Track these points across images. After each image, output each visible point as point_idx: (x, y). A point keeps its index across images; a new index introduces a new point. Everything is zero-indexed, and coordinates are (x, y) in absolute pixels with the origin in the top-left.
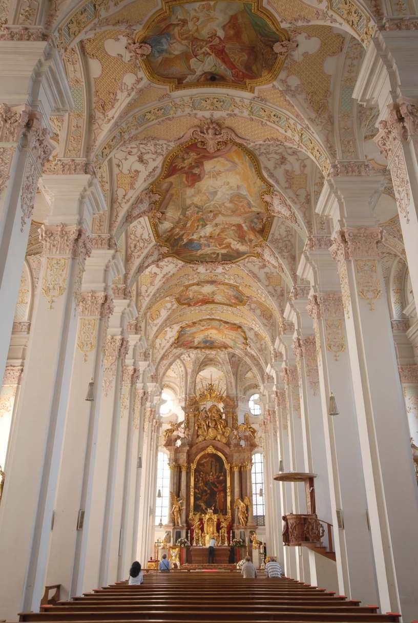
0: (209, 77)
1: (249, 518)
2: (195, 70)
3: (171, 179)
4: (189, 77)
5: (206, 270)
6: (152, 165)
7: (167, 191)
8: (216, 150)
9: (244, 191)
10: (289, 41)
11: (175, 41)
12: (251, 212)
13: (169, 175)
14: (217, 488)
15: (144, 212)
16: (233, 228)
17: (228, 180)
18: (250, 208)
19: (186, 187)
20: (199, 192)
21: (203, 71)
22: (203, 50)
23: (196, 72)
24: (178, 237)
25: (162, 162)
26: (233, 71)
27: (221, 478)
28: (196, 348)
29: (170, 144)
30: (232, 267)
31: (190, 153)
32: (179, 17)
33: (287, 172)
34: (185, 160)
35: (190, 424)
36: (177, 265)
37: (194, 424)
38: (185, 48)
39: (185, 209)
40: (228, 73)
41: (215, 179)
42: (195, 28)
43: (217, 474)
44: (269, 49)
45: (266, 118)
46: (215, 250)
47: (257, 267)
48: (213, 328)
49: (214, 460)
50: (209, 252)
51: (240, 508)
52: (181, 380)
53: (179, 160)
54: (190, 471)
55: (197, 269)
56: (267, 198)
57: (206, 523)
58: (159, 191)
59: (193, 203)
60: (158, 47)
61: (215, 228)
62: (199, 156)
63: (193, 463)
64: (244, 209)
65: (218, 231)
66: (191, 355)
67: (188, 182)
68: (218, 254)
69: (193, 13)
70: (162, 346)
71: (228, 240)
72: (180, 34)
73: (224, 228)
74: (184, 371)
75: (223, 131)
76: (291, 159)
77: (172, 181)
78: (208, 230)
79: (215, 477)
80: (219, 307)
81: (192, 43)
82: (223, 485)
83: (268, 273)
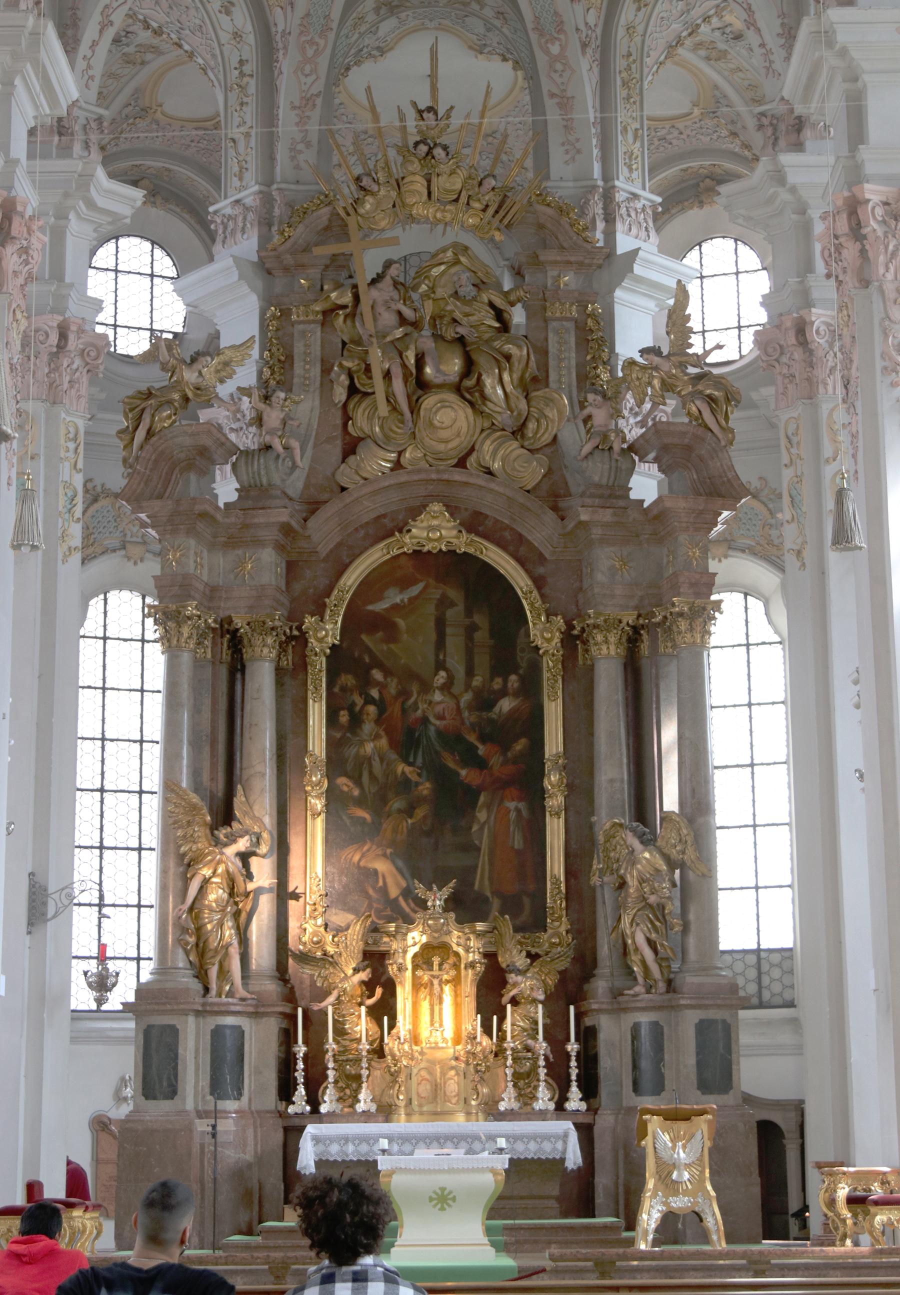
1: (691, 941)
14: (481, 764)
27: (506, 705)
35: (298, 368)
37: (326, 370)
43: (477, 681)
49: (455, 594)
51: (632, 883)
52: (233, 97)
54: (302, 665)
57: (409, 974)
63: (320, 610)
74: (251, 39)
79: (467, 697)
82: (520, 745)
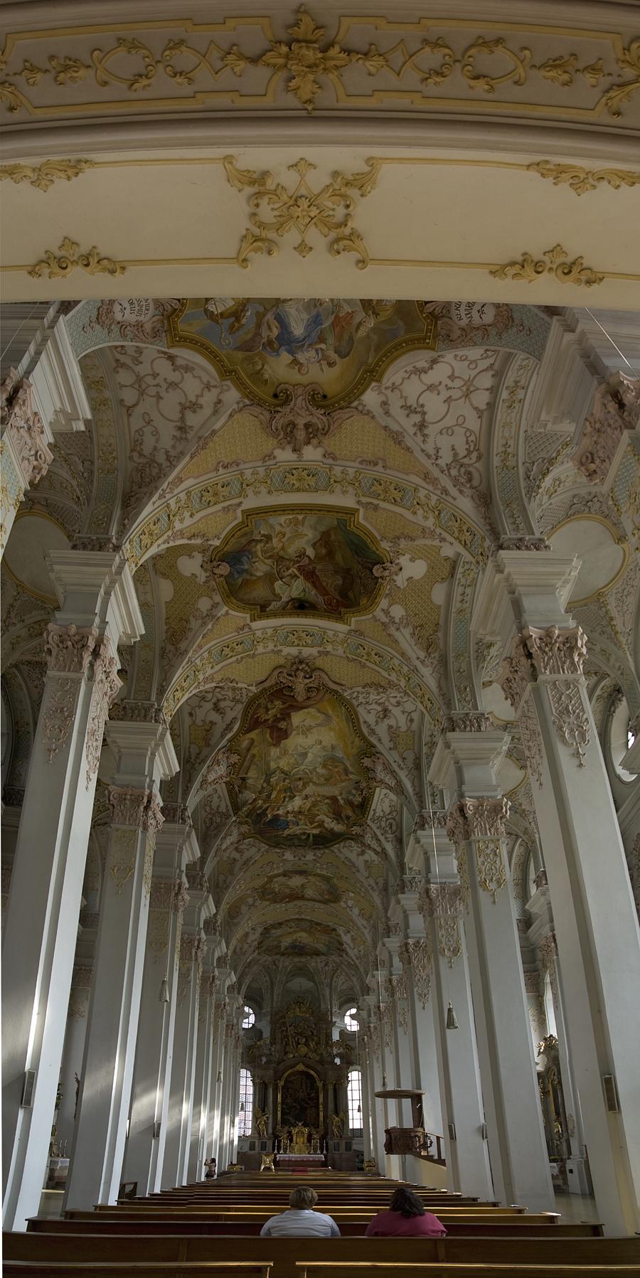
0: (297, 605)
2: (282, 595)
3: (253, 735)
4: (274, 603)
5: (295, 857)
6: (230, 715)
7: (249, 750)
10: (391, 563)
11: (257, 559)
12: (349, 780)
13: (249, 731)
15: (221, 777)
16: (326, 801)
17: (321, 738)
19: (270, 746)
20: (285, 752)
21: (290, 596)
22: (290, 571)
23: (281, 598)
24: (260, 811)
26: (325, 597)
28: (283, 954)
29: (250, 688)
32: (262, 532)
33: (390, 727)
36: (259, 850)
38: (269, 568)
39: (269, 775)
40: (321, 599)
41: (304, 736)
42: (281, 545)
44: (368, 572)
45: (365, 657)
48: (305, 931)
50: (298, 832)
53: (262, 710)
55: (284, 855)
56: (367, 762)
58: (238, 750)
59: (278, 767)
60: (238, 566)
61: (305, 801)
64: (339, 776)
65: (308, 805)
66: (276, 962)
67: (272, 739)
68: (309, 835)
69: (278, 528)
70: (244, 950)
71: (321, 817)
72: (264, 552)
75: (316, 673)
76: (396, 711)
77: (254, 738)
78: (297, 803)
80: (310, 904)
81: (277, 563)
83: (366, 861)
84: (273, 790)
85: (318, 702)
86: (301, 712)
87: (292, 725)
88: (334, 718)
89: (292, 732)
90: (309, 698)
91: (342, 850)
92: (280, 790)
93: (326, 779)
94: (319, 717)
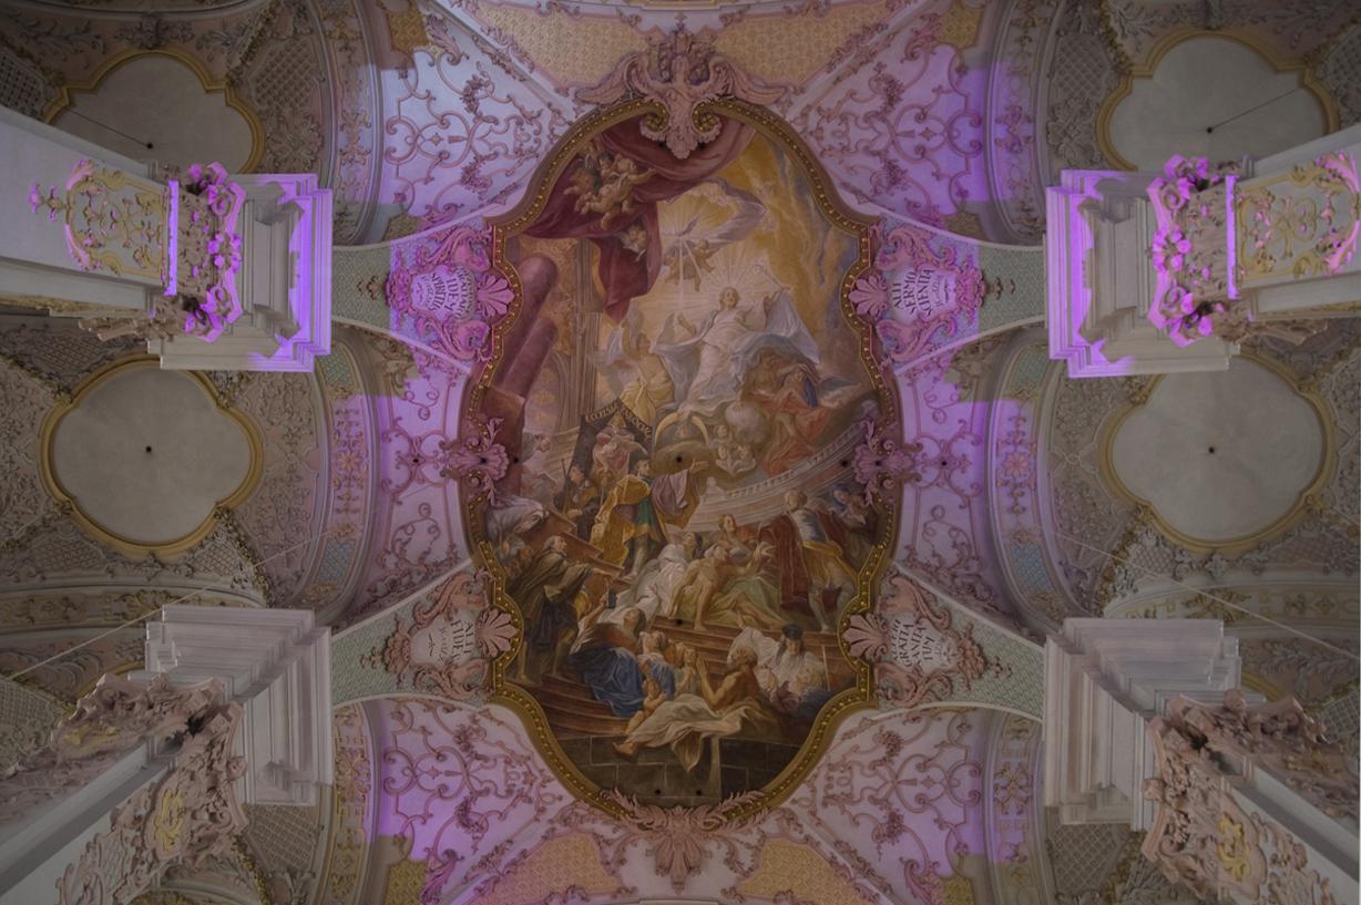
3: (557, 250)
8: (694, 146)
9: (789, 316)
17: (734, 283)
18: (815, 403)
25: (533, 172)
30: (764, 836)
31: (618, 156)
34: (601, 185)
36: (541, 811)
39: (591, 429)
41: (691, 284)
46: (695, 715)
47: (866, 827)
50: (674, 731)
55: (622, 862)
59: (618, 402)
62: (642, 176)
65: (705, 582)
68: (707, 741)
73: (729, 561)
77: (560, 269)
83: (910, 865)
84: (597, 501)
85: (725, 161)
86: (683, 199)
87: (660, 249)
88: (769, 200)
89: (659, 269)
90: (702, 147)
91: (822, 813)
92: (619, 506)
93: (758, 450)
94: (728, 207)
